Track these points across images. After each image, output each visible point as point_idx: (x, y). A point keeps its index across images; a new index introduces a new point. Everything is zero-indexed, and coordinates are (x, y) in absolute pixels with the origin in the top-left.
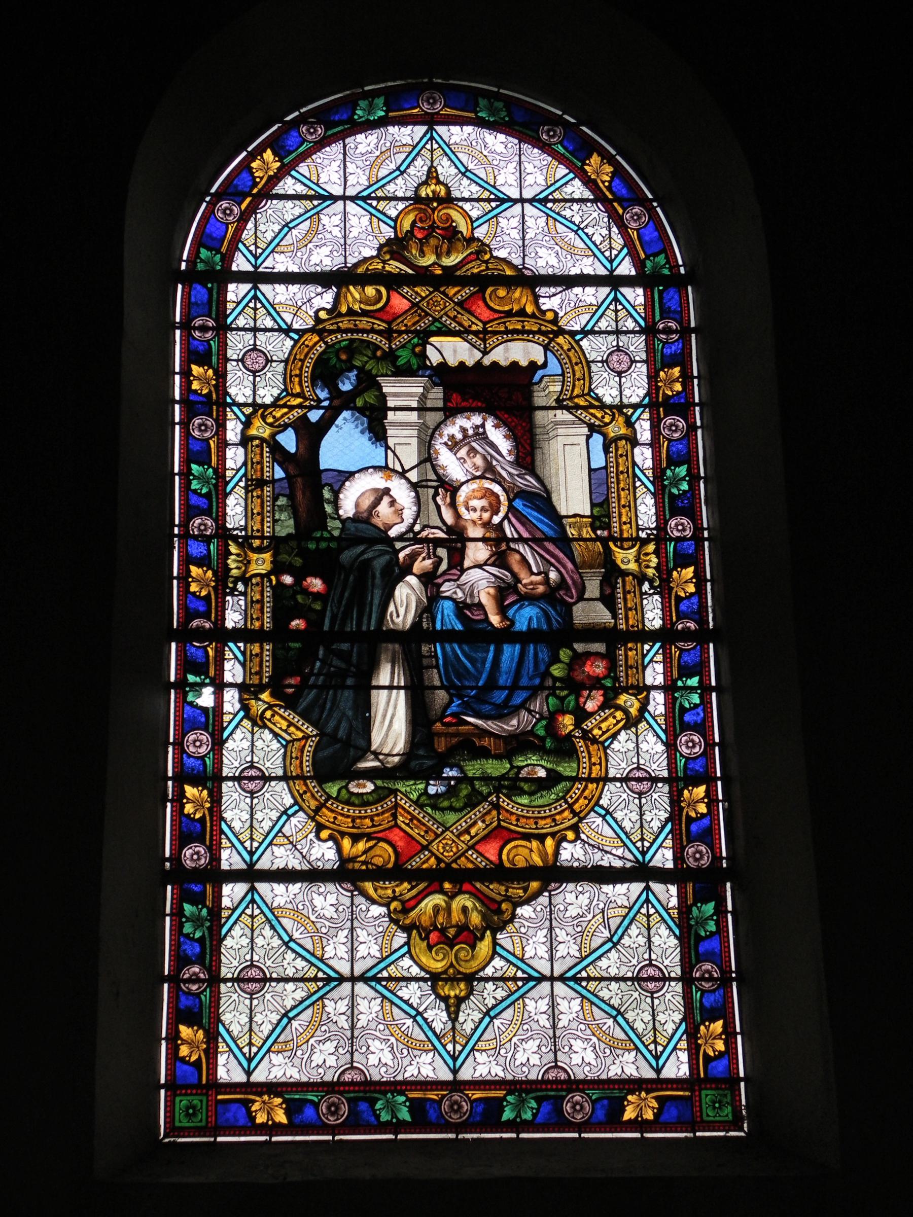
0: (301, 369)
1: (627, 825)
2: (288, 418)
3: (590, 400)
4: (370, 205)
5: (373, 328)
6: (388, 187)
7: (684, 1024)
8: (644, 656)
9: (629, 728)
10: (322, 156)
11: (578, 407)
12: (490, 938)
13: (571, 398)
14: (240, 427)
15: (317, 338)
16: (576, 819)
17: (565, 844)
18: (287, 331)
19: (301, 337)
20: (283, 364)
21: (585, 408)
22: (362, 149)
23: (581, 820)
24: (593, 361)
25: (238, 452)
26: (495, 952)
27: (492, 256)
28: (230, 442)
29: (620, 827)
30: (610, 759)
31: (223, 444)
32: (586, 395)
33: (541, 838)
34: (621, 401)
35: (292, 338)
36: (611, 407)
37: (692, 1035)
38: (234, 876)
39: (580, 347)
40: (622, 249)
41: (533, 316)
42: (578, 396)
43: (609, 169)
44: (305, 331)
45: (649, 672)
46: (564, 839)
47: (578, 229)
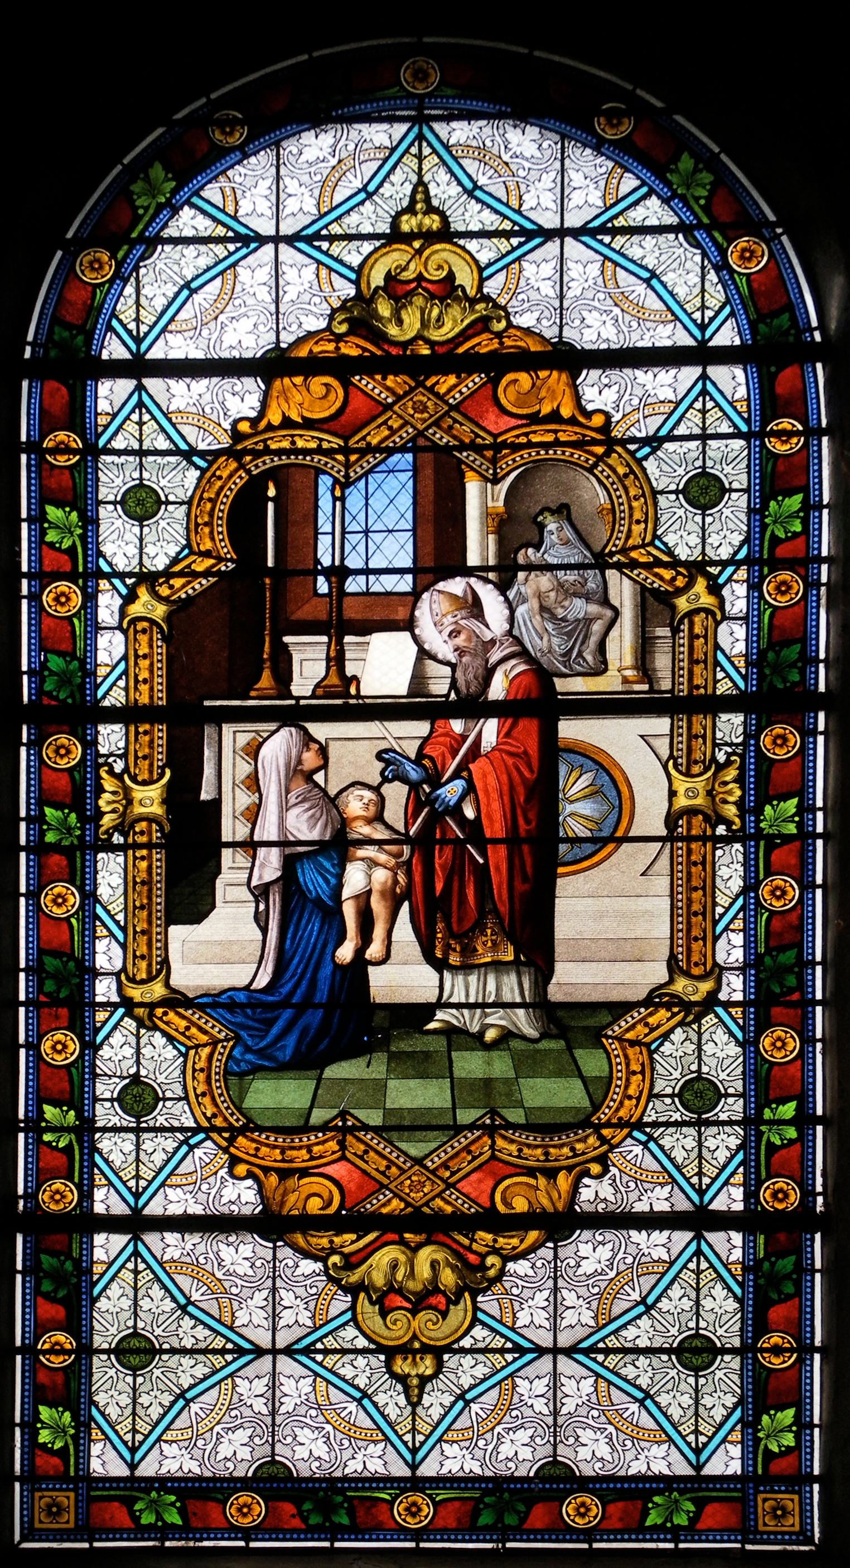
0: (211, 514)
1: (679, 1155)
2: (193, 588)
3: (655, 552)
4: (319, 249)
5: (320, 446)
6: (346, 220)
7: (739, 1409)
8: (715, 923)
9: (689, 1024)
10: (243, 171)
11: (634, 564)
12: (469, 1303)
13: (624, 551)
14: (118, 601)
15: (234, 465)
16: (605, 1147)
17: (586, 1181)
18: (189, 454)
19: (211, 464)
20: (184, 507)
21: (647, 566)
22: (310, 155)
23: (612, 1147)
24: (662, 492)
25: (115, 641)
26: (475, 1321)
27: (510, 325)
28: (103, 625)
29: (668, 1157)
30: (658, 1067)
31: (95, 627)
32: (648, 545)
33: (551, 1174)
34: (703, 553)
35: (197, 467)
36: (686, 564)
37: (750, 1425)
38: (111, 1224)
39: (644, 470)
40: (722, 308)
41: (572, 421)
42: (635, 548)
43: (706, 177)
44: (217, 454)
45: (721, 943)
46: (587, 1173)
47: (651, 278)
